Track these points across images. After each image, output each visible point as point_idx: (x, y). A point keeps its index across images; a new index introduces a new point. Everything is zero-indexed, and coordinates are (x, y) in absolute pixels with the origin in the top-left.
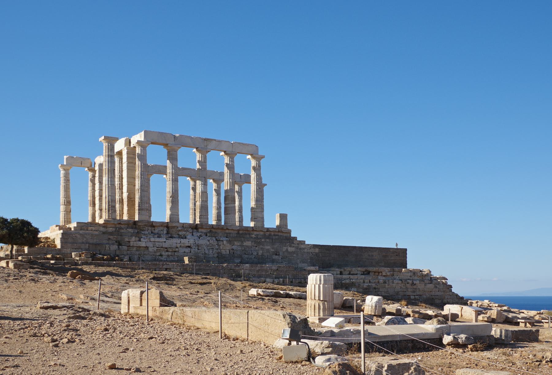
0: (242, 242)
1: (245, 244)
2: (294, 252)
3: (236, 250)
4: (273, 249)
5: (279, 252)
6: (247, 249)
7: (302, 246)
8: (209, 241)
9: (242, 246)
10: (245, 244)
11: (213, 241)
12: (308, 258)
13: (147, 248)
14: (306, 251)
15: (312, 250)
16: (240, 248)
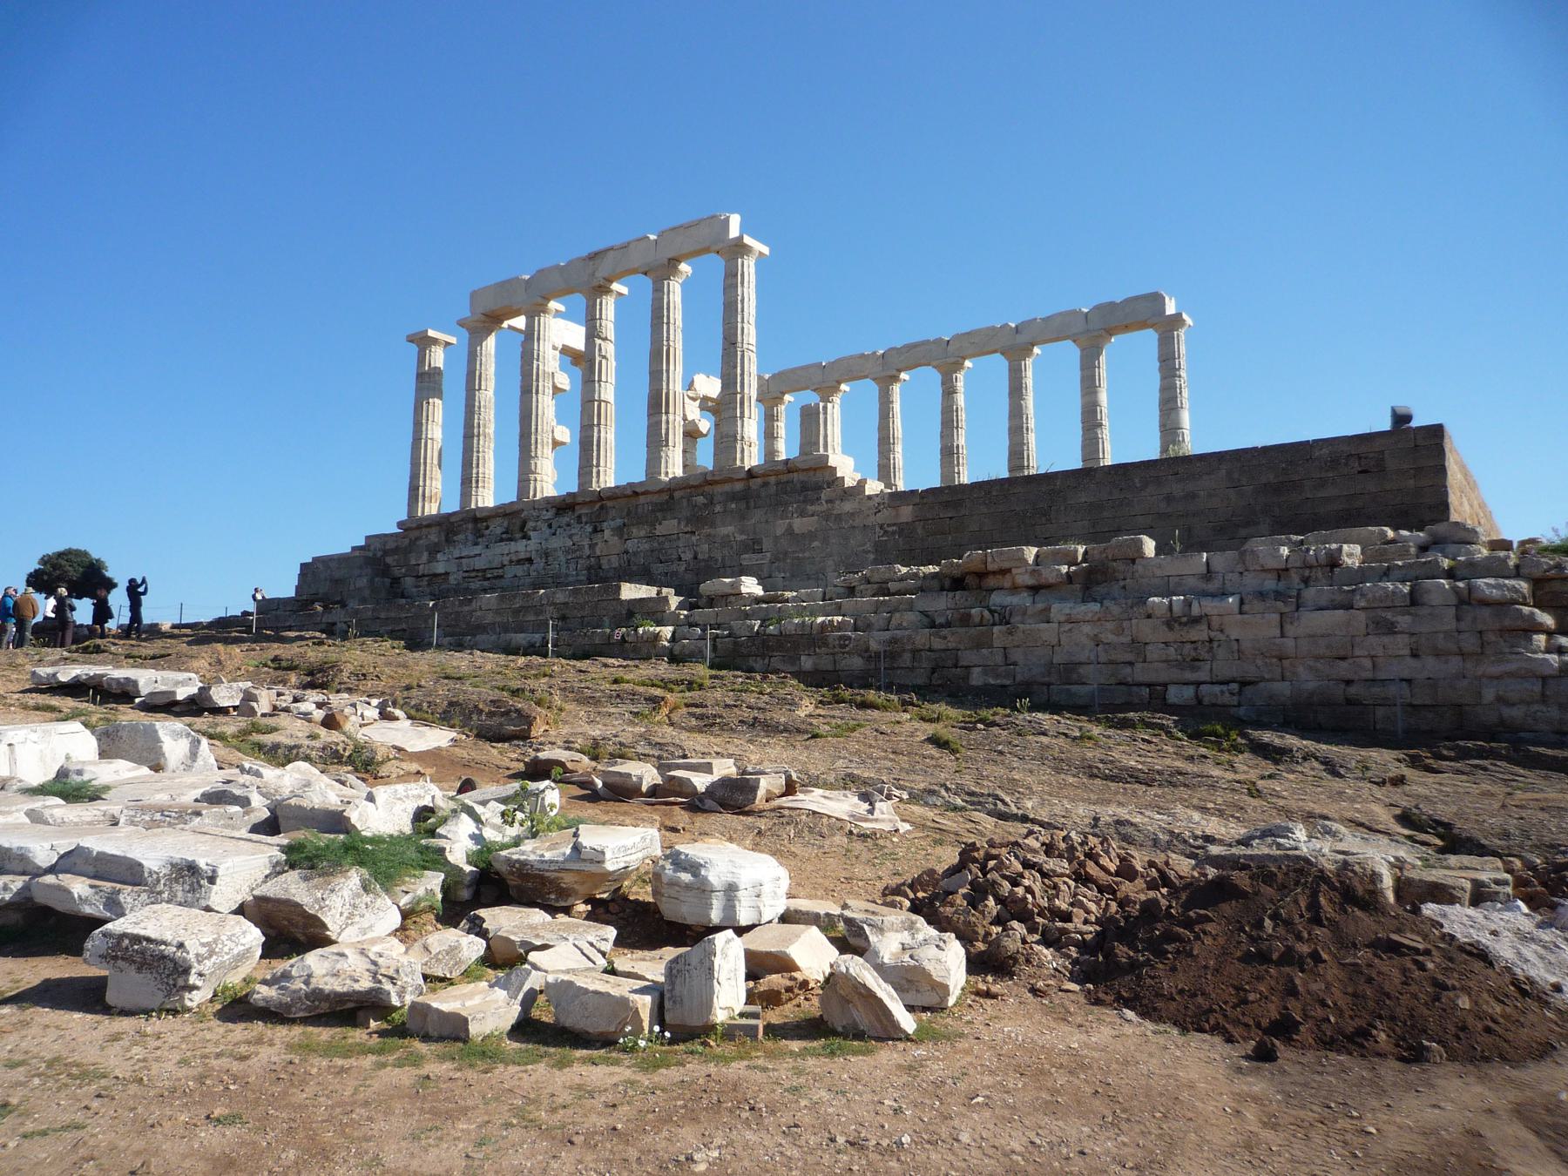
0: (653, 525)
1: (659, 530)
2: (812, 536)
3: (635, 554)
4: (742, 532)
5: (759, 542)
6: (667, 545)
7: (848, 507)
8: (570, 537)
9: (651, 537)
10: (659, 530)
11: (581, 535)
12: (868, 547)
13: (447, 574)
14: (858, 522)
15: (885, 516)
16: (647, 546)
